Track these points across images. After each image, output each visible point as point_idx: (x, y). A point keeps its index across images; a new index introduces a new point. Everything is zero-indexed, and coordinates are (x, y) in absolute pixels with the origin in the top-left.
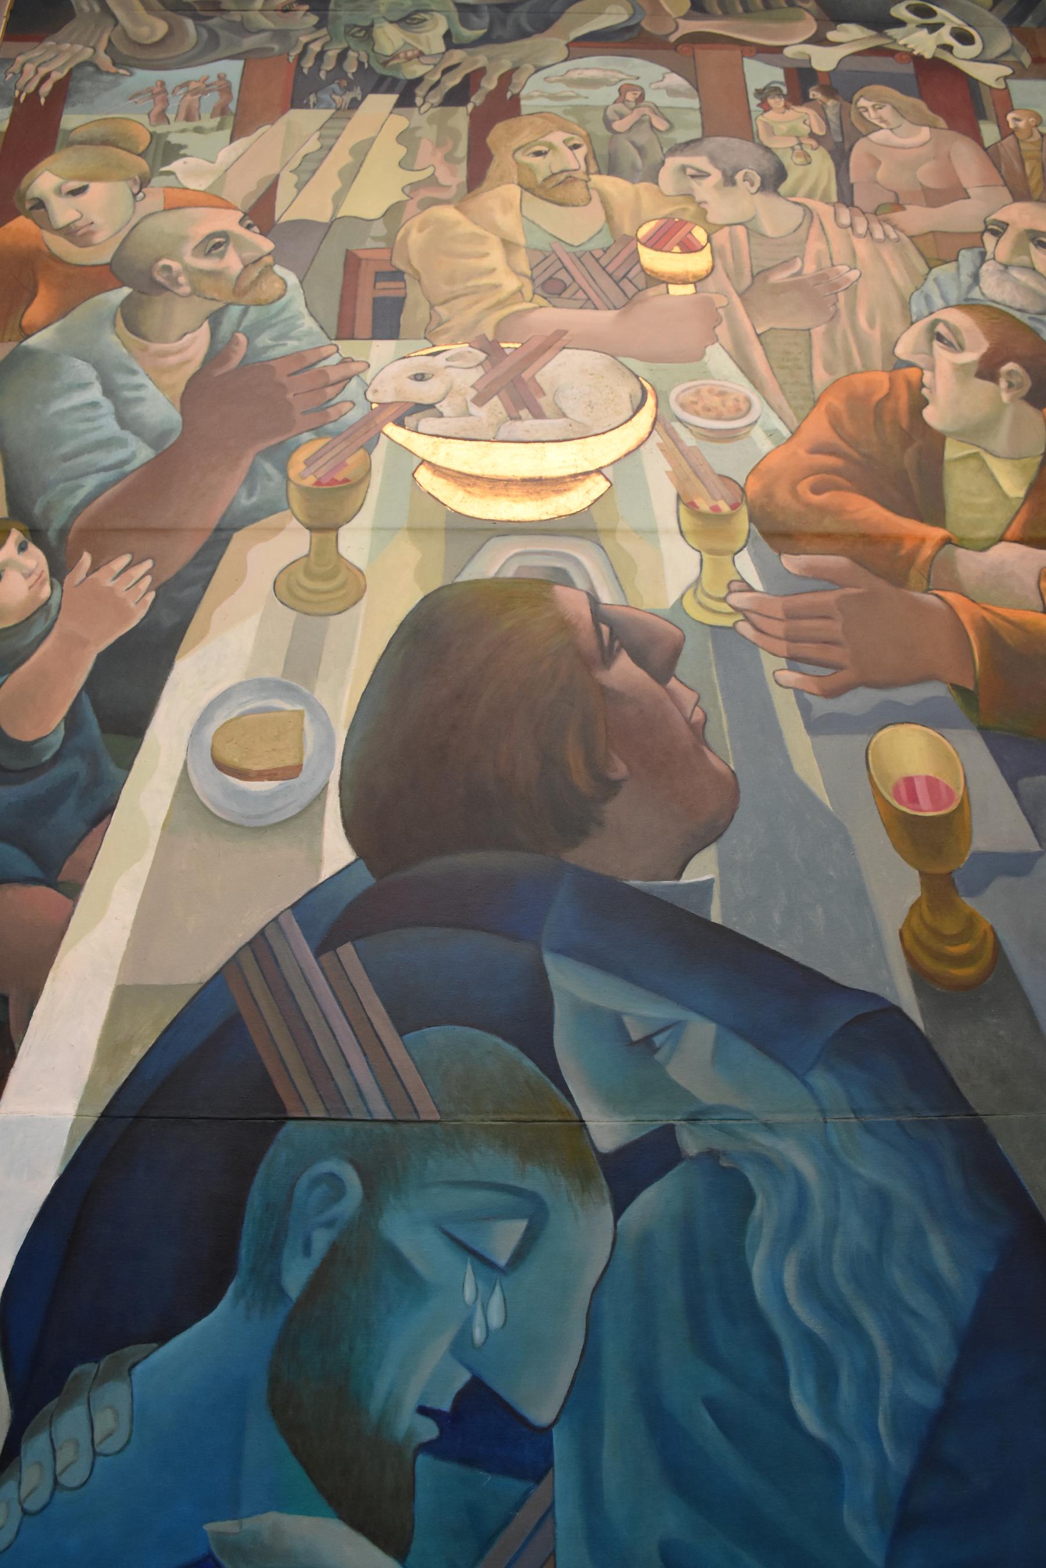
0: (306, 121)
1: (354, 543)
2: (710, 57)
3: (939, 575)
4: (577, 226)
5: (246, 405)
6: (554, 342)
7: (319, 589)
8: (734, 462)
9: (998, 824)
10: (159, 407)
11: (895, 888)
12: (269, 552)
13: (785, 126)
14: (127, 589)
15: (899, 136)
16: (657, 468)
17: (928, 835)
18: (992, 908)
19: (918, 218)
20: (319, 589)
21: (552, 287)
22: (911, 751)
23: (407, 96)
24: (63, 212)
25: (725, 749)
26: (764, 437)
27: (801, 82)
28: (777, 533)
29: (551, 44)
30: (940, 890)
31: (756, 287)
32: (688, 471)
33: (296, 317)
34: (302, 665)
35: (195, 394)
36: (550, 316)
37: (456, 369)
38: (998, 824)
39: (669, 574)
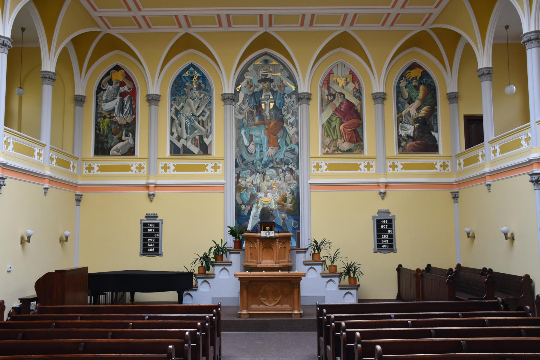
0: (254, 175)
1: (259, 205)
2: (277, 169)
3: (286, 206)
4: (269, 184)
5: (253, 197)
6: (268, 193)
7: (257, 207)
8: (276, 200)
9: (287, 218)
10: (249, 197)
11: (282, 221)
12: (255, 205)
13: (281, 175)
14: (249, 207)
15: (288, 175)
16: (273, 200)
17: (284, 219)
18: (286, 222)
19: (288, 182)
20: (257, 207)
21: (268, 189)
22: (283, 215)
23: (259, 173)
24: (241, 183)
25: (275, 215)
26: (278, 198)
27: (283, 170)
28: (278, 204)
29: (268, 168)
30: (284, 221)
31: (279, 188)
32: (274, 200)
33: (255, 192)
34: (257, 211)
35: (250, 196)
36: (268, 191)
37: (263, 195)
38: (287, 218)
39: (273, 206)
